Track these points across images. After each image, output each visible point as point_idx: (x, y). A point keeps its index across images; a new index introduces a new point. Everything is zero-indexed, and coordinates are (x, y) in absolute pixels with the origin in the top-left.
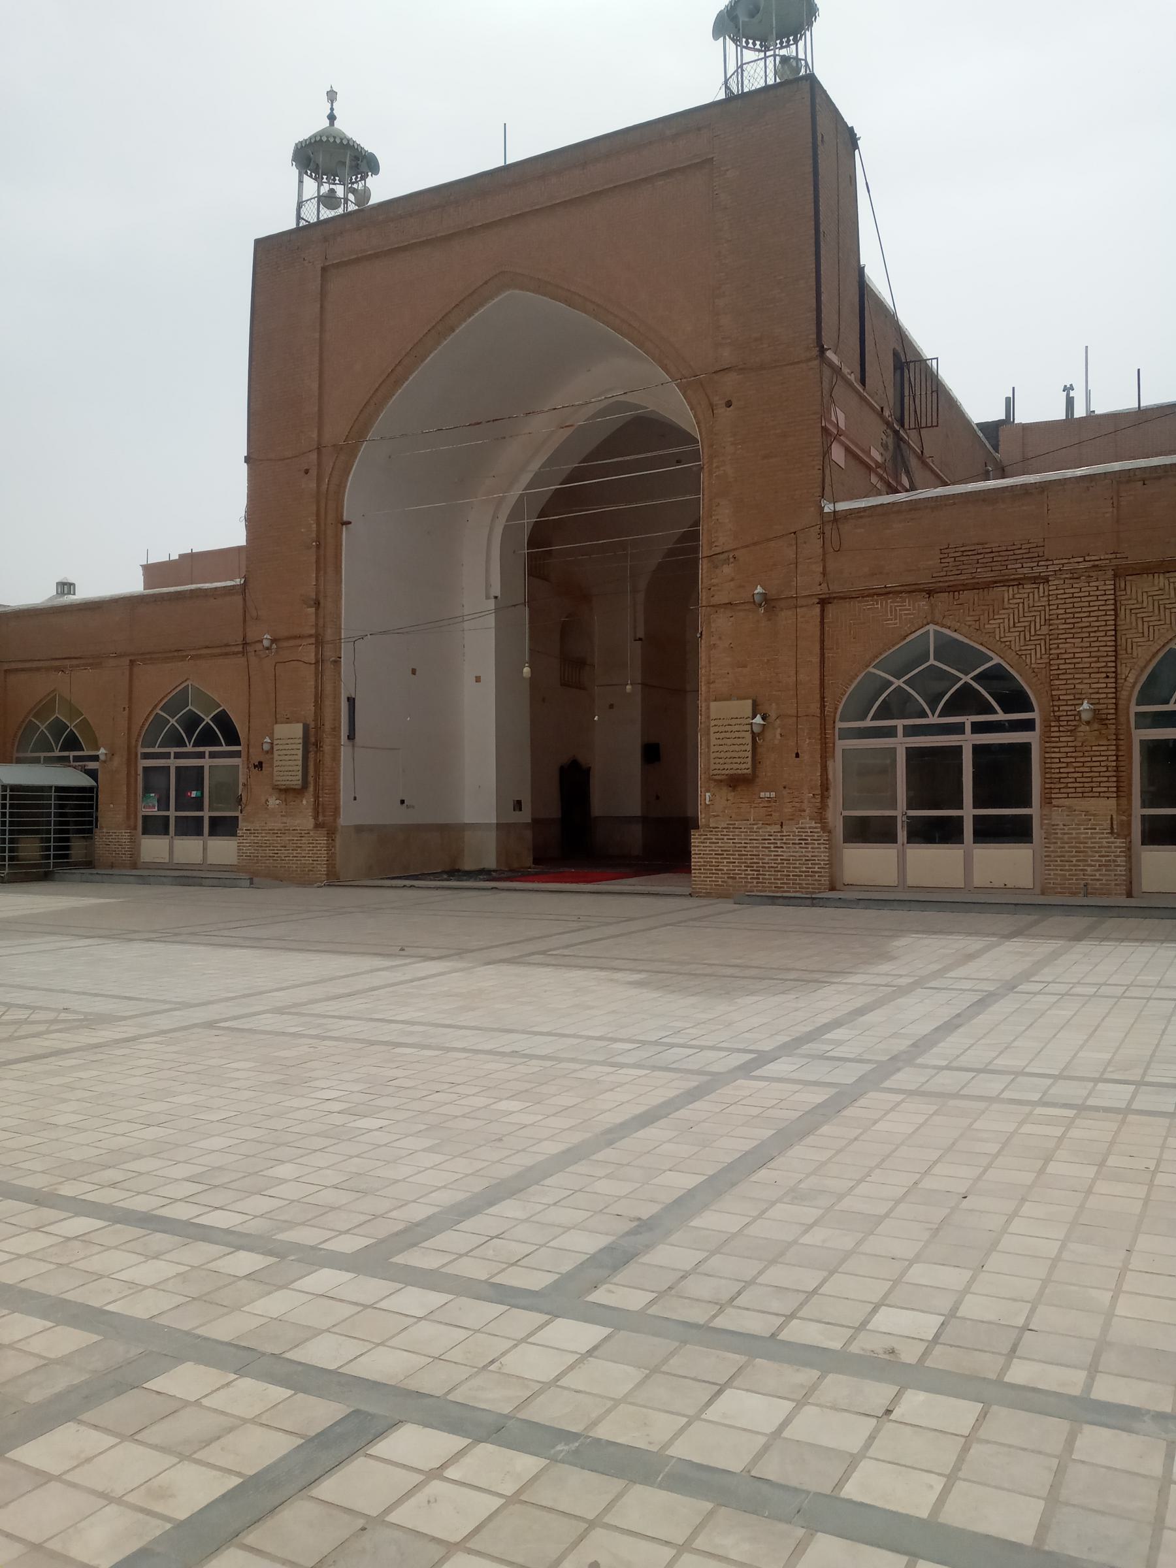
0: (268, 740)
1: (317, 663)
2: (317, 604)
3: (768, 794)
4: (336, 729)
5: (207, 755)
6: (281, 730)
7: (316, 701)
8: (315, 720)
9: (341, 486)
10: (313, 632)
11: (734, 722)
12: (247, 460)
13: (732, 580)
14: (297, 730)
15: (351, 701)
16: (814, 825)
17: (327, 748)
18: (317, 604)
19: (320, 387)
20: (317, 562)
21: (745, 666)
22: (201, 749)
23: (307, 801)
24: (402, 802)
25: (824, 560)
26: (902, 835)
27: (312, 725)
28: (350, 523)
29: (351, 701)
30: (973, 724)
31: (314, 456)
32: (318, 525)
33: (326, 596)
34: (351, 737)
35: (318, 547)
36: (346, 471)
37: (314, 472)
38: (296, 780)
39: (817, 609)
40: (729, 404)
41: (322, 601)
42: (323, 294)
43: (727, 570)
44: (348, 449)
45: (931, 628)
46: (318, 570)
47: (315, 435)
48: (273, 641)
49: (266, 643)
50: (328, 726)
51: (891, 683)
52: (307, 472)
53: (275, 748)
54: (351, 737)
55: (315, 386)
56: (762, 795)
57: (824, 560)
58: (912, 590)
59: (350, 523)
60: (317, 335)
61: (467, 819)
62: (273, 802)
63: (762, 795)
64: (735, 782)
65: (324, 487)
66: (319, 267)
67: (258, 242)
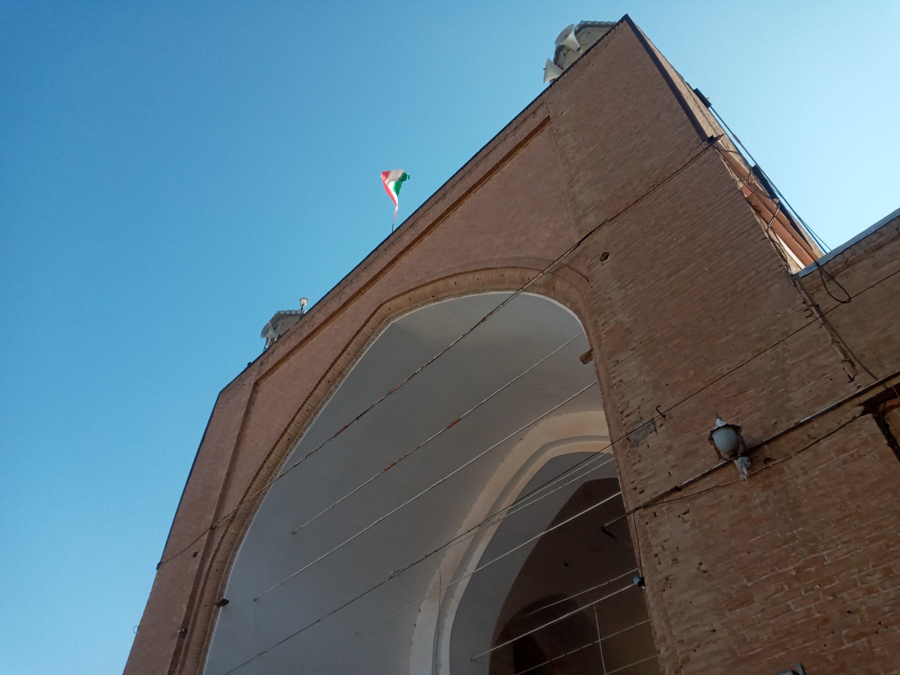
9: (226, 563)
12: (159, 566)
13: (670, 448)
19: (229, 474)
20: (177, 653)
21: (748, 601)
25: (837, 339)
28: (225, 602)
31: (206, 537)
35: (183, 635)
36: (234, 546)
37: (200, 554)
39: (870, 424)
40: (605, 256)
42: (251, 401)
43: (653, 440)
44: (241, 519)
46: (174, 664)
47: (210, 517)
52: (195, 555)
55: (223, 474)
57: (837, 339)
59: (225, 602)
66: (252, 383)
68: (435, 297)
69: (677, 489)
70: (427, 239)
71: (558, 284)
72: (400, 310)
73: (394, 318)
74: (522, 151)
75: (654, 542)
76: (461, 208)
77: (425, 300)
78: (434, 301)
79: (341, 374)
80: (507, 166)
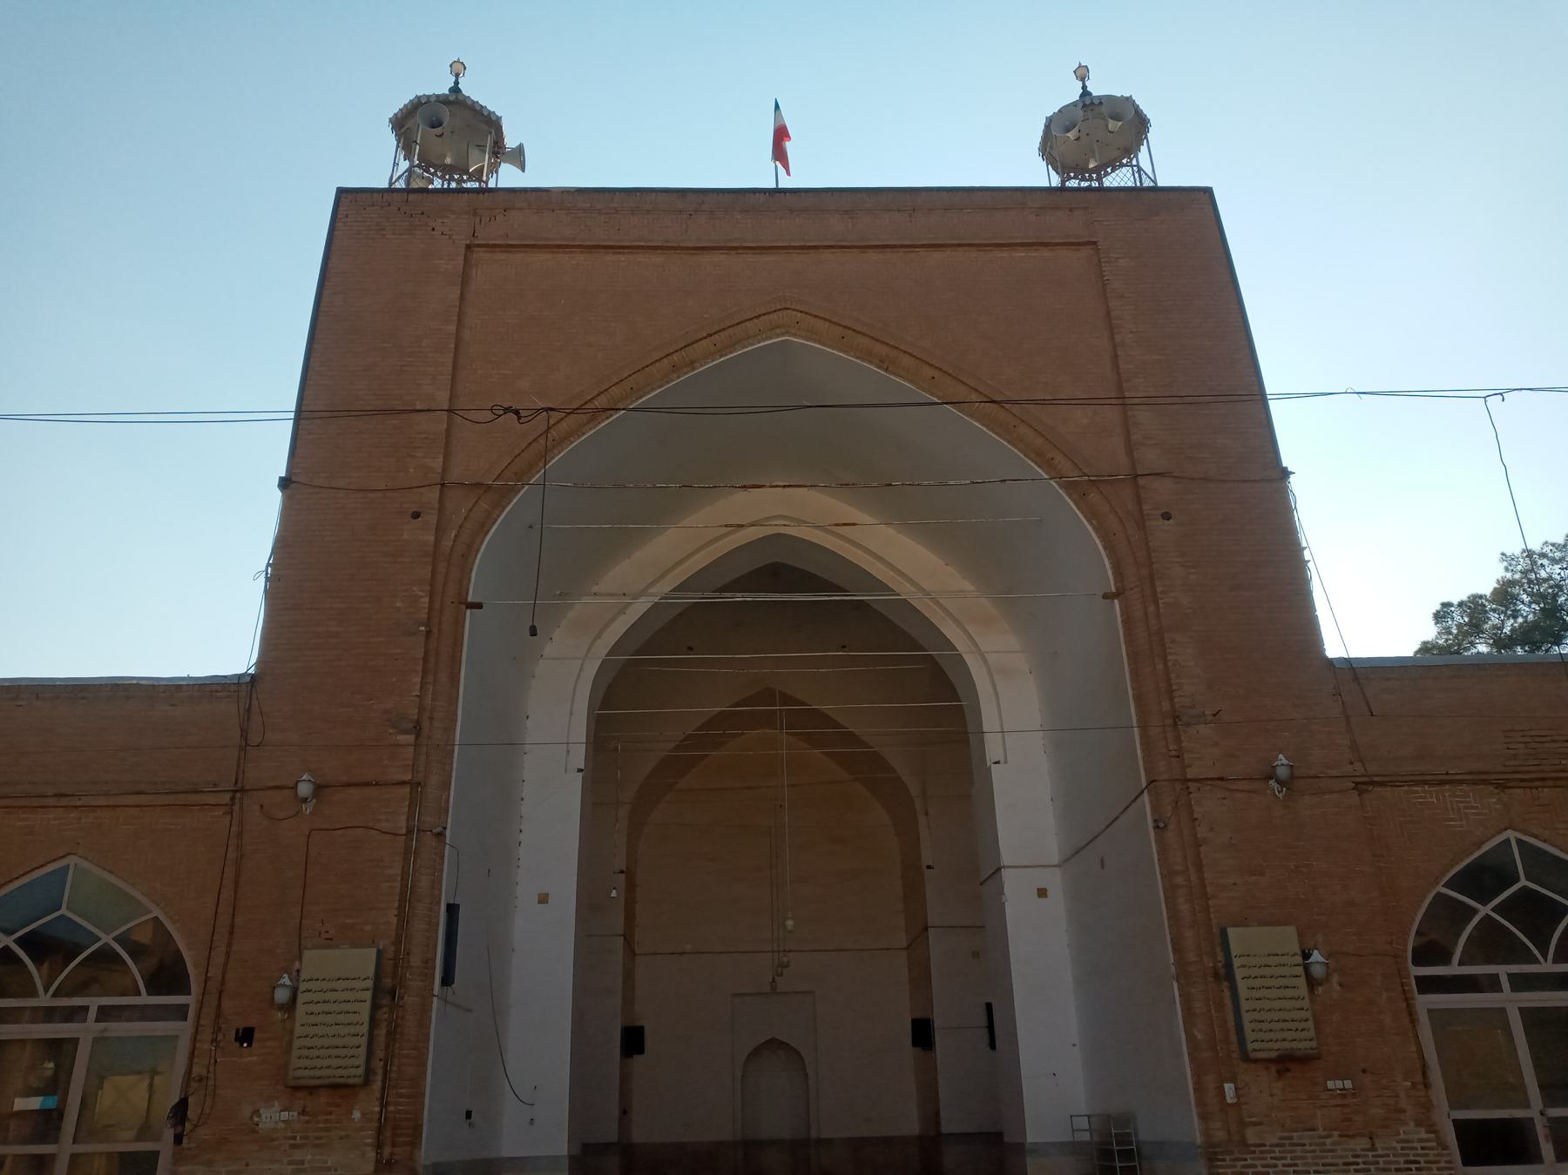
0: (286, 980)
1: (409, 832)
2: (417, 729)
3: (1339, 1084)
4: (428, 963)
5: (92, 1014)
6: (316, 961)
7: (401, 908)
8: (397, 943)
9: (471, 549)
10: (408, 777)
11: (1272, 960)
12: (284, 483)
14: (362, 962)
15: (452, 910)
16: (1424, 1135)
17: (410, 1000)
18: (417, 729)
22: (77, 1001)
23: (362, 1111)
24: (469, 1115)
26: (1547, 1149)
27: (390, 954)
29: (452, 910)
30: (1511, 976)
31: (433, 495)
32: (432, 595)
33: (431, 719)
34: (447, 980)
35: (428, 634)
36: (483, 528)
37: (432, 519)
38: (352, 1066)
40: (1167, 516)
41: (425, 724)
42: (465, 282)
44: (495, 493)
45: (1511, 835)
47: (437, 464)
48: (319, 789)
49: (304, 789)
50: (415, 961)
51: (1475, 911)
53: (301, 998)
54: (447, 980)
56: (1330, 1084)
58: (1479, 779)
59: (479, 606)
60: (452, 328)
61: (506, 1153)
62: (273, 1116)
63: (1330, 1084)
64: (1286, 1063)
65: (447, 543)
67: (342, 192)
68: (882, 363)
69: (1221, 779)
70: (872, 256)
71: (1094, 496)
72: (812, 334)
73: (794, 335)
74: (1046, 253)
75: (1196, 808)
76: (937, 255)
77: (867, 355)
78: (879, 367)
79: (692, 364)
80: (1020, 253)
